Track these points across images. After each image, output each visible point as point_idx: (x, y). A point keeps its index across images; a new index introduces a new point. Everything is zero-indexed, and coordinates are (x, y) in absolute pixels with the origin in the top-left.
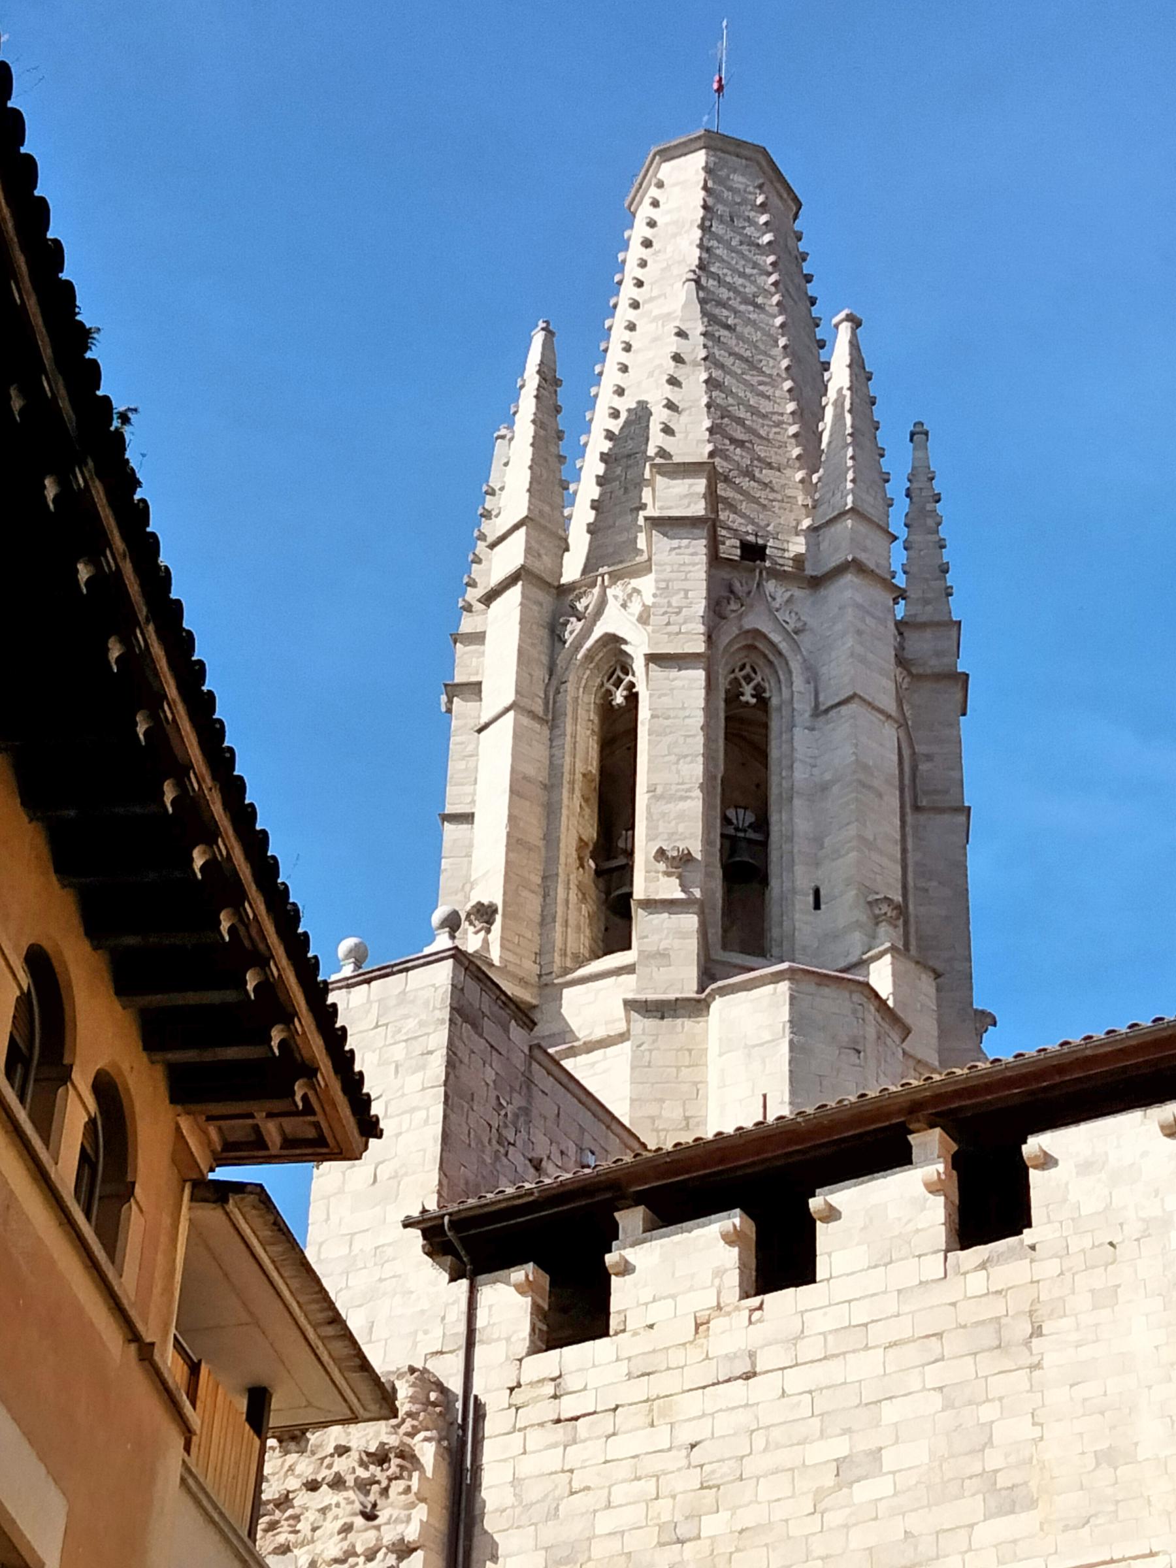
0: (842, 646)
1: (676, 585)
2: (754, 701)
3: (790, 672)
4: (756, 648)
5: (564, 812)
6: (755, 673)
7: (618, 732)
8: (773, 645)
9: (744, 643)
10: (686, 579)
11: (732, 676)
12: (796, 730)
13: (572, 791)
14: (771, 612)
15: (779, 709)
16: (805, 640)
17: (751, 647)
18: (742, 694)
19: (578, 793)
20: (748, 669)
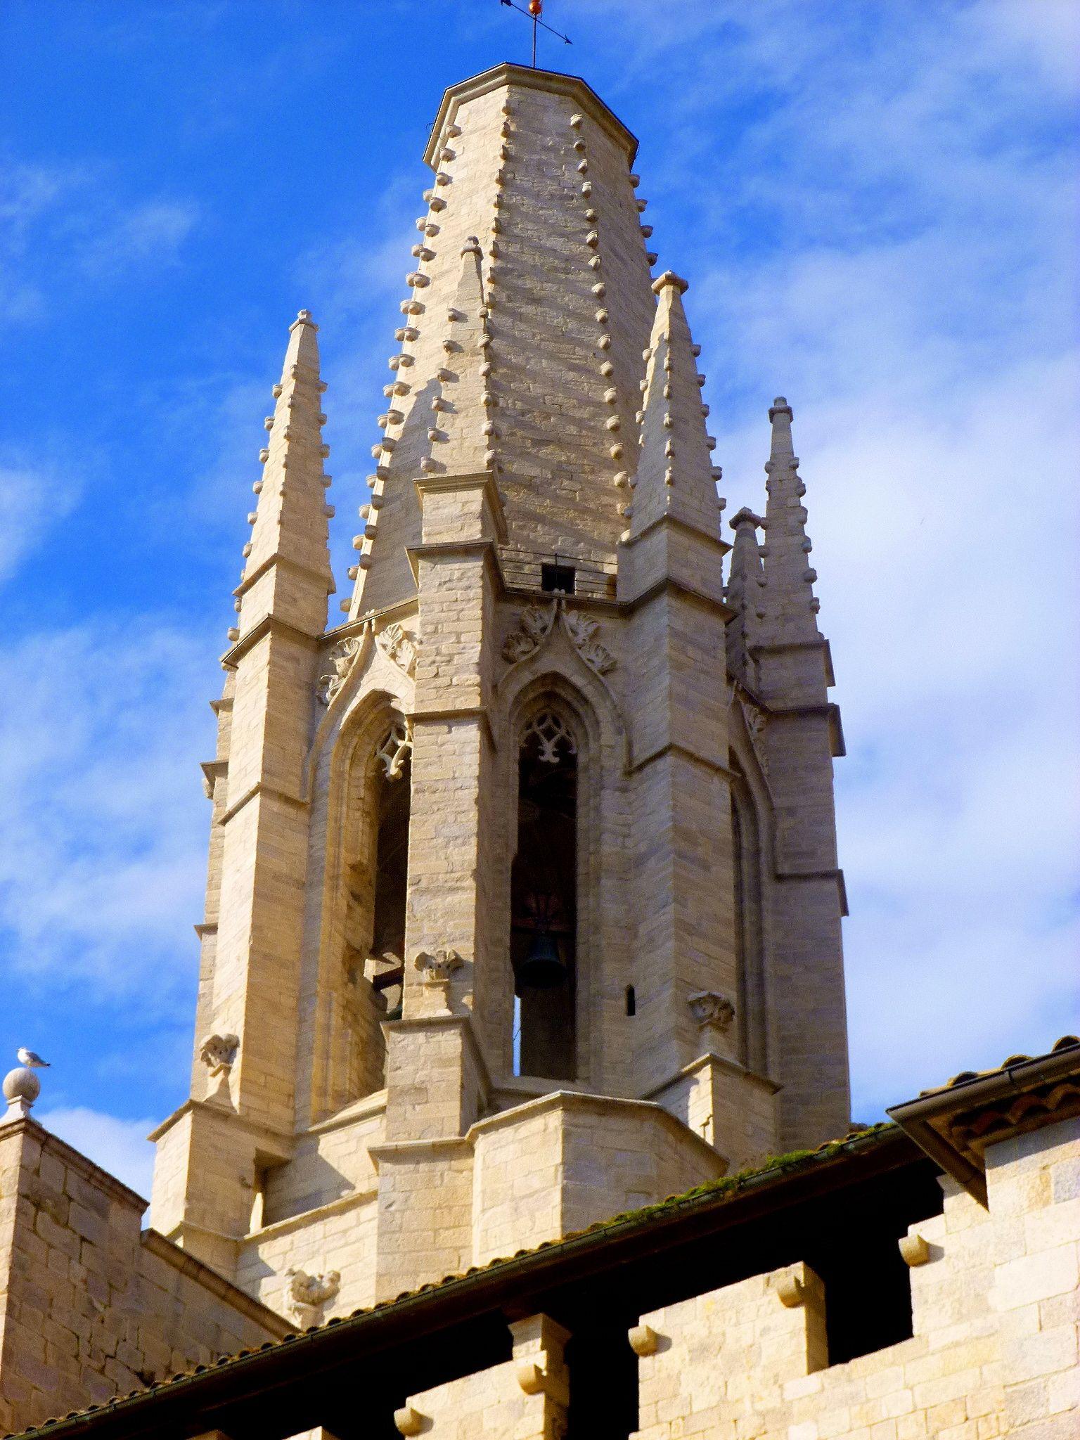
0: (660, 689)
2: (556, 760)
3: (597, 723)
5: (325, 915)
6: (559, 726)
7: (391, 807)
9: (542, 690)
10: (458, 619)
12: (607, 794)
13: (335, 888)
14: (573, 648)
15: (587, 769)
16: (616, 682)
17: (551, 696)
18: (543, 753)
19: (343, 890)
20: (549, 722)
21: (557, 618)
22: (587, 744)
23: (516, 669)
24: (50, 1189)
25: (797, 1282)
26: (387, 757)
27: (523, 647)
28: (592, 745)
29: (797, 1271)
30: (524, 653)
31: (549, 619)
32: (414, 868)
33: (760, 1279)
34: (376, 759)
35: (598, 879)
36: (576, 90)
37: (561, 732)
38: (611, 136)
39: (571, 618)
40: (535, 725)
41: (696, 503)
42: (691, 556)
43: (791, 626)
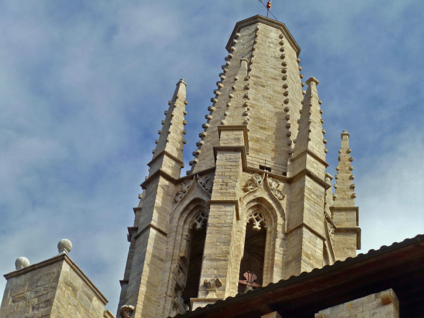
1: (227, 174)
2: (260, 228)
4: (262, 206)
6: (261, 217)
8: (269, 204)
10: (231, 171)
11: (250, 218)
18: (255, 225)
20: (258, 215)
21: (265, 180)
22: (271, 224)
23: (249, 194)
24: (71, 283)
25: (390, 294)
26: (197, 222)
27: (251, 187)
28: (273, 224)
29: (389, 293)
30: (251, 189)
31: (261, 179)
32: (207, 252)
33: (373, 295)
34: (193, 223)
35: (272, 268)
36: (282, 27)
37: (262, 220)
38: (291, 45)
39: (269, 180)
40: (253, 216)
41: (318, 149)
42: (315, 165)
43: (346, 201)
